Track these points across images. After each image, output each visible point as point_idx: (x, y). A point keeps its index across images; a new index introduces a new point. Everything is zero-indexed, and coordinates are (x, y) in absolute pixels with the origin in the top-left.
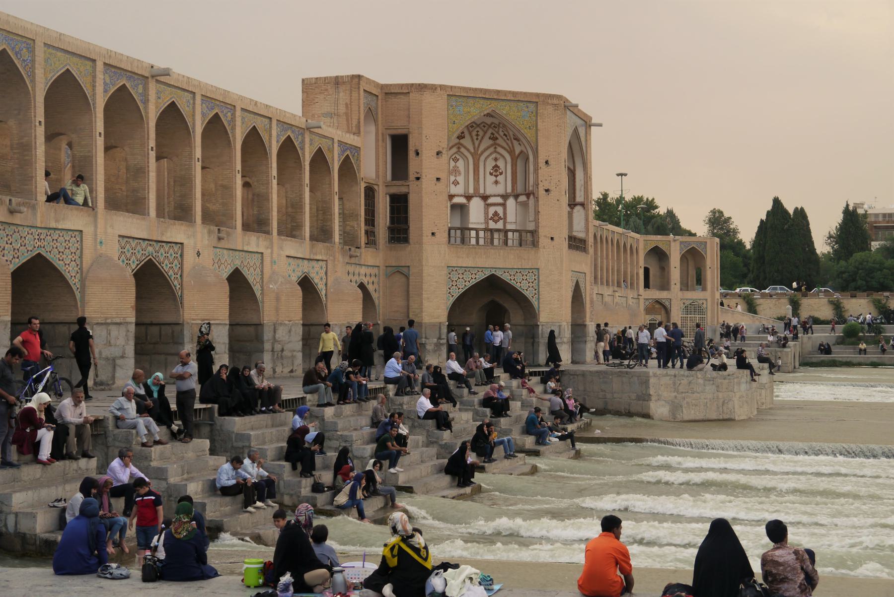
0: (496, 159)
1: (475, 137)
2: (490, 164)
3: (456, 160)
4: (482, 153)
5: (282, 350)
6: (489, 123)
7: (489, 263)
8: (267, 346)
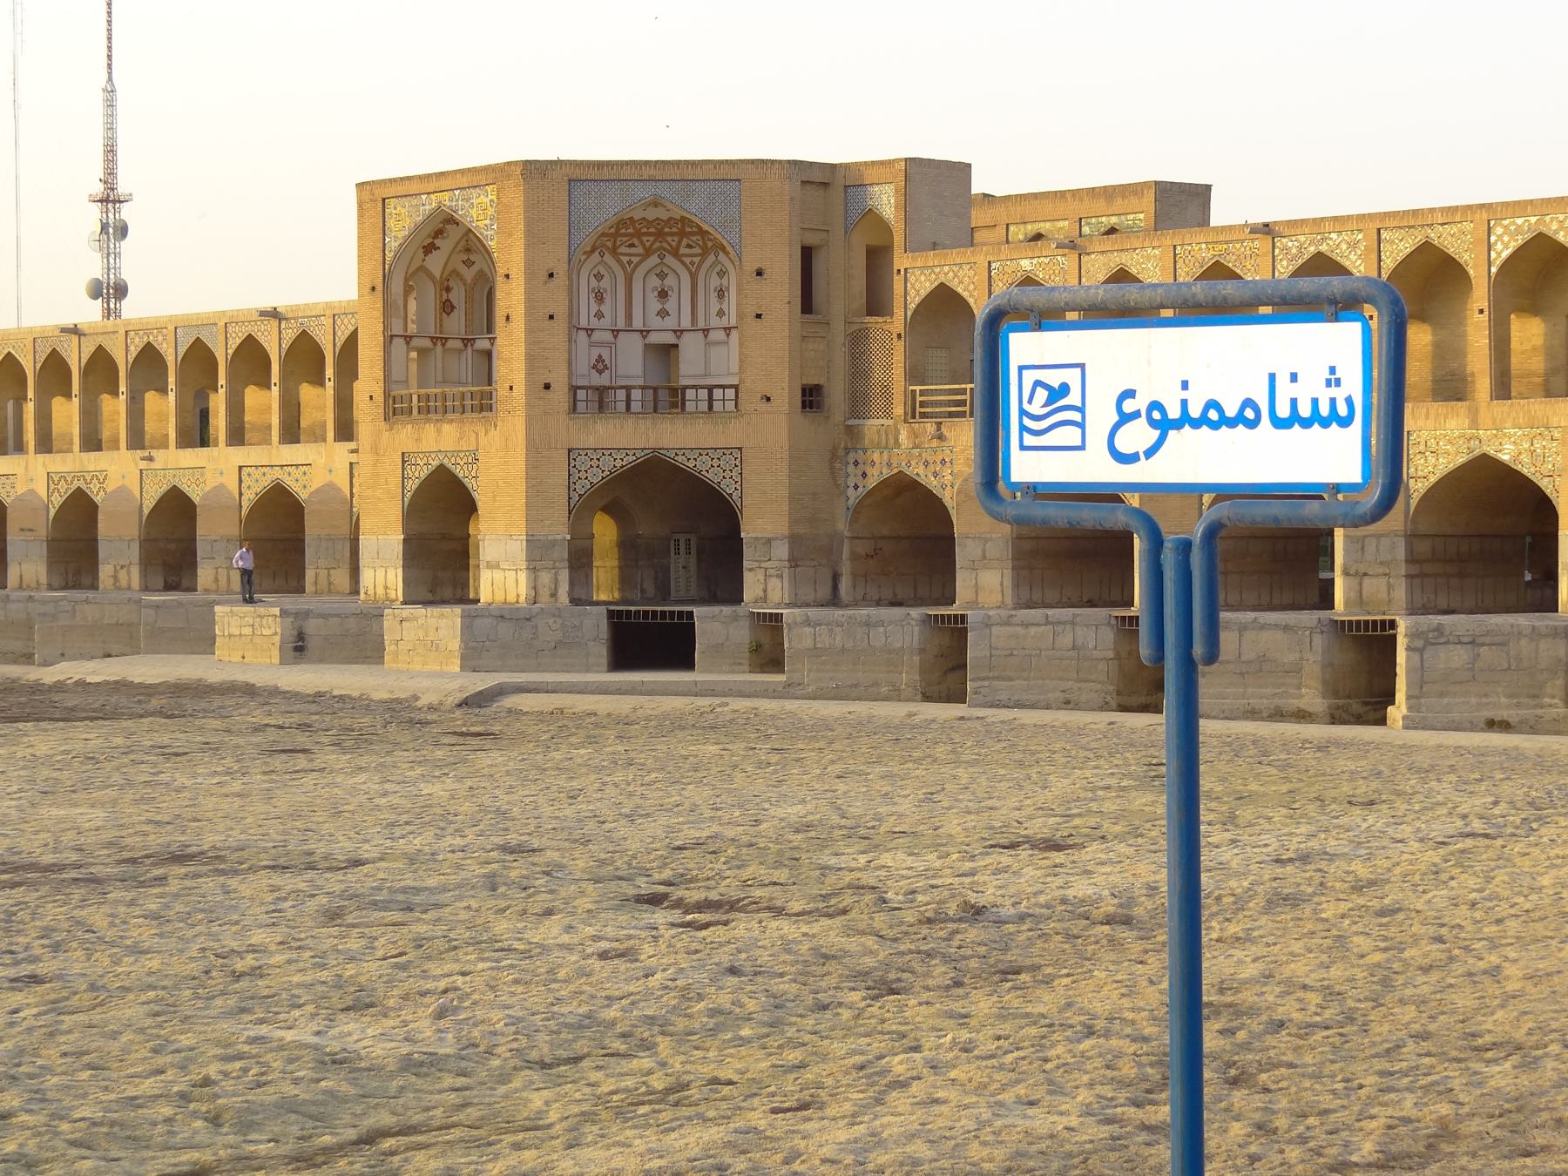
0: (662, 276)
3: (599, 277)
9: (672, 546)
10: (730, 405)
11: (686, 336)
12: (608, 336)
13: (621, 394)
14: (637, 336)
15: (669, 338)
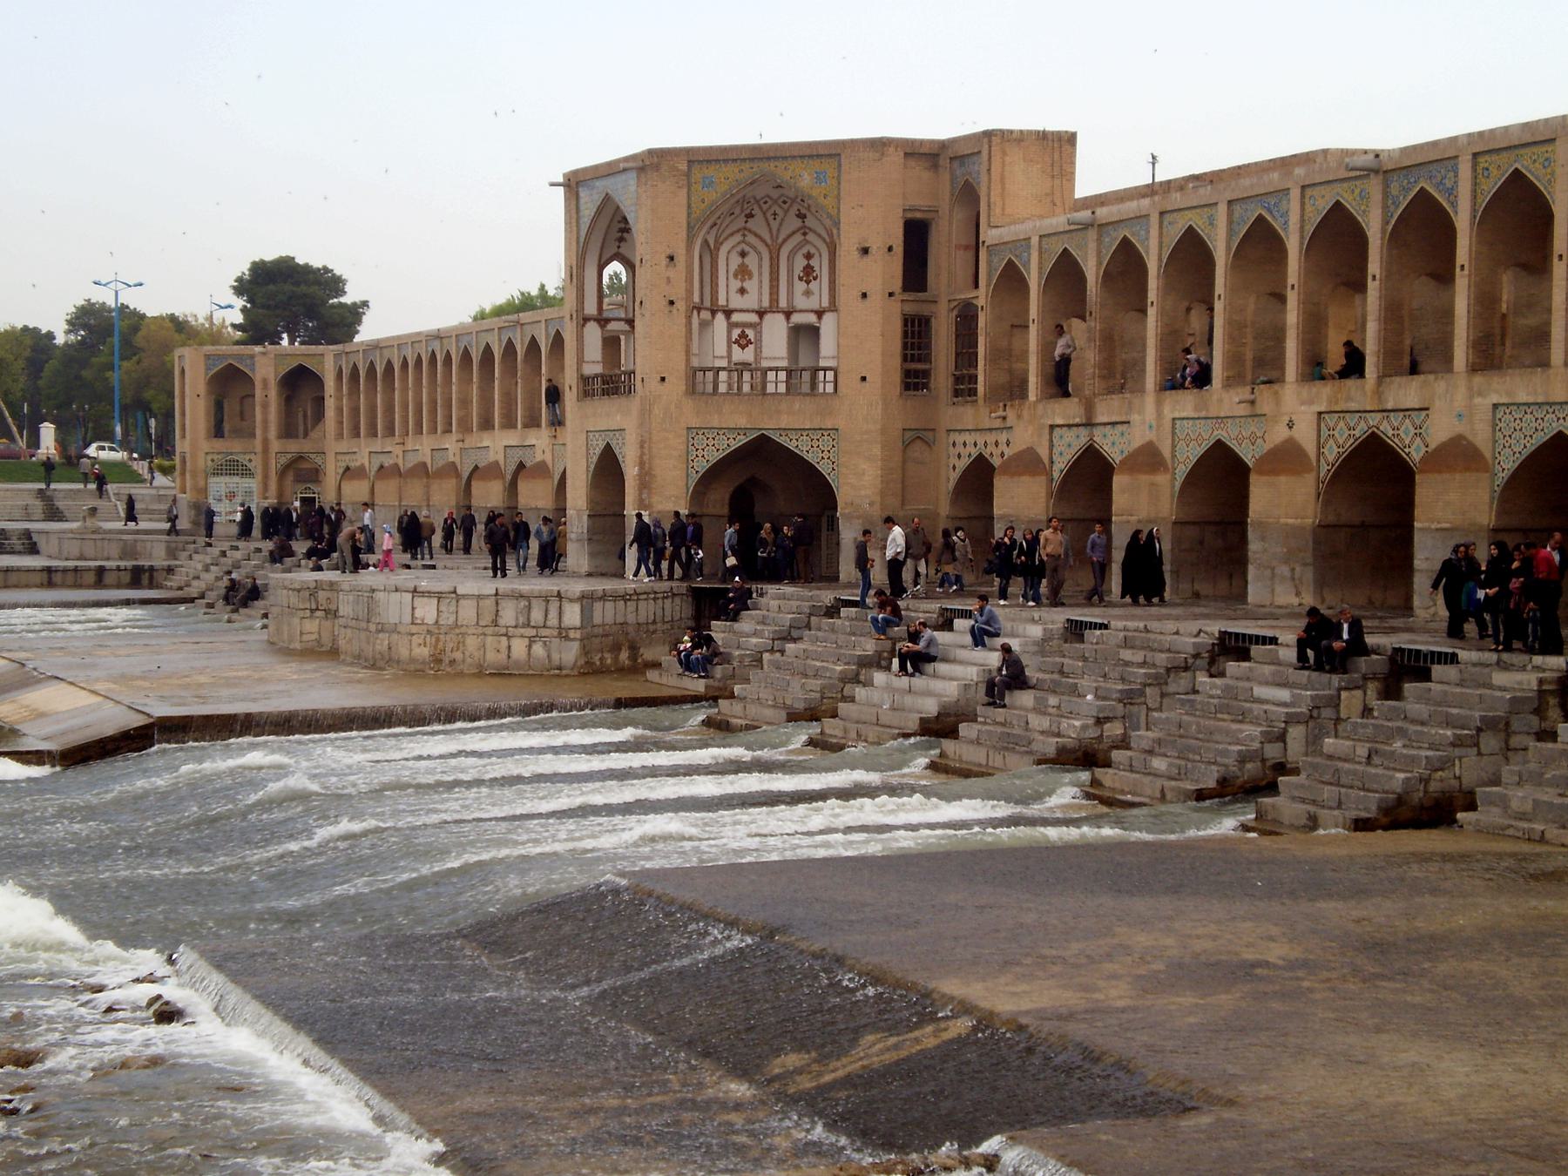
0: (808, 256)
1: (771, 218)
2: (800, 263)
3: (743, 254)
4: (785, 241)
6: (775, 197)
9: (824, 526)
10: (830, 388)
11: (828, 318)
12: (754, 318)
13: (710, 375)
14: (781, 317)
15: (812, 318)
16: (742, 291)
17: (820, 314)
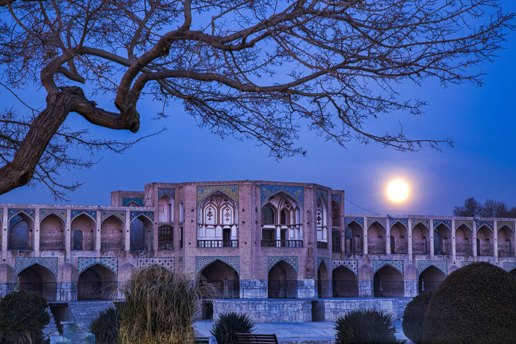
0: (228, 210)
1: (218, 201)
3: (210, 209)
4: (221, 206)
5: (64, 292)
7: (215, 255)
8: (58, 290)
12: (213, 227)
15: (229, 227)
16: (210, 219)
17: (231, 226)
